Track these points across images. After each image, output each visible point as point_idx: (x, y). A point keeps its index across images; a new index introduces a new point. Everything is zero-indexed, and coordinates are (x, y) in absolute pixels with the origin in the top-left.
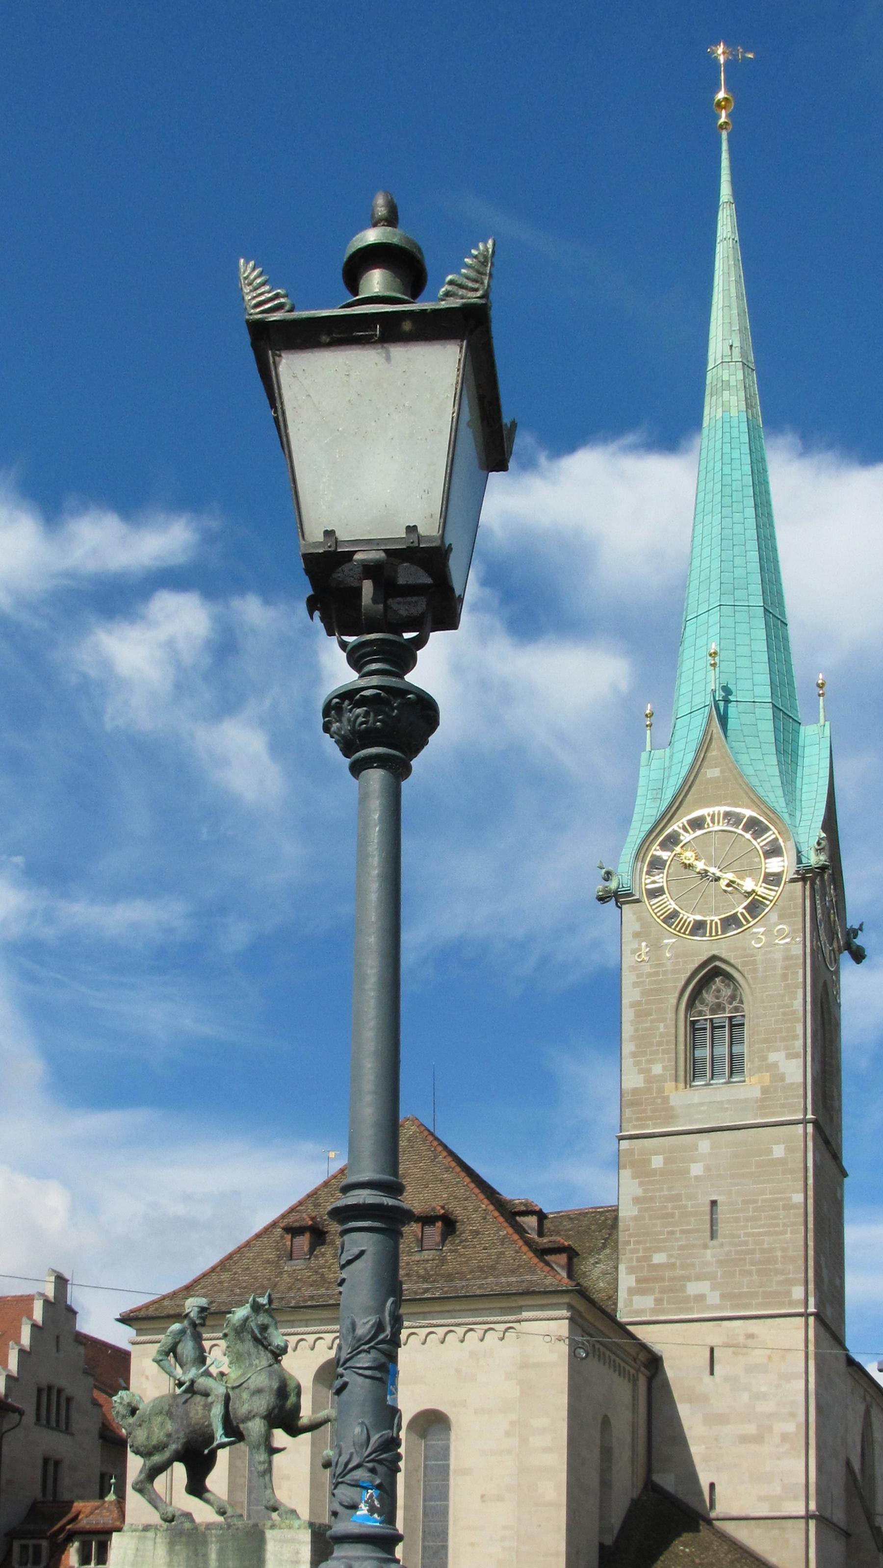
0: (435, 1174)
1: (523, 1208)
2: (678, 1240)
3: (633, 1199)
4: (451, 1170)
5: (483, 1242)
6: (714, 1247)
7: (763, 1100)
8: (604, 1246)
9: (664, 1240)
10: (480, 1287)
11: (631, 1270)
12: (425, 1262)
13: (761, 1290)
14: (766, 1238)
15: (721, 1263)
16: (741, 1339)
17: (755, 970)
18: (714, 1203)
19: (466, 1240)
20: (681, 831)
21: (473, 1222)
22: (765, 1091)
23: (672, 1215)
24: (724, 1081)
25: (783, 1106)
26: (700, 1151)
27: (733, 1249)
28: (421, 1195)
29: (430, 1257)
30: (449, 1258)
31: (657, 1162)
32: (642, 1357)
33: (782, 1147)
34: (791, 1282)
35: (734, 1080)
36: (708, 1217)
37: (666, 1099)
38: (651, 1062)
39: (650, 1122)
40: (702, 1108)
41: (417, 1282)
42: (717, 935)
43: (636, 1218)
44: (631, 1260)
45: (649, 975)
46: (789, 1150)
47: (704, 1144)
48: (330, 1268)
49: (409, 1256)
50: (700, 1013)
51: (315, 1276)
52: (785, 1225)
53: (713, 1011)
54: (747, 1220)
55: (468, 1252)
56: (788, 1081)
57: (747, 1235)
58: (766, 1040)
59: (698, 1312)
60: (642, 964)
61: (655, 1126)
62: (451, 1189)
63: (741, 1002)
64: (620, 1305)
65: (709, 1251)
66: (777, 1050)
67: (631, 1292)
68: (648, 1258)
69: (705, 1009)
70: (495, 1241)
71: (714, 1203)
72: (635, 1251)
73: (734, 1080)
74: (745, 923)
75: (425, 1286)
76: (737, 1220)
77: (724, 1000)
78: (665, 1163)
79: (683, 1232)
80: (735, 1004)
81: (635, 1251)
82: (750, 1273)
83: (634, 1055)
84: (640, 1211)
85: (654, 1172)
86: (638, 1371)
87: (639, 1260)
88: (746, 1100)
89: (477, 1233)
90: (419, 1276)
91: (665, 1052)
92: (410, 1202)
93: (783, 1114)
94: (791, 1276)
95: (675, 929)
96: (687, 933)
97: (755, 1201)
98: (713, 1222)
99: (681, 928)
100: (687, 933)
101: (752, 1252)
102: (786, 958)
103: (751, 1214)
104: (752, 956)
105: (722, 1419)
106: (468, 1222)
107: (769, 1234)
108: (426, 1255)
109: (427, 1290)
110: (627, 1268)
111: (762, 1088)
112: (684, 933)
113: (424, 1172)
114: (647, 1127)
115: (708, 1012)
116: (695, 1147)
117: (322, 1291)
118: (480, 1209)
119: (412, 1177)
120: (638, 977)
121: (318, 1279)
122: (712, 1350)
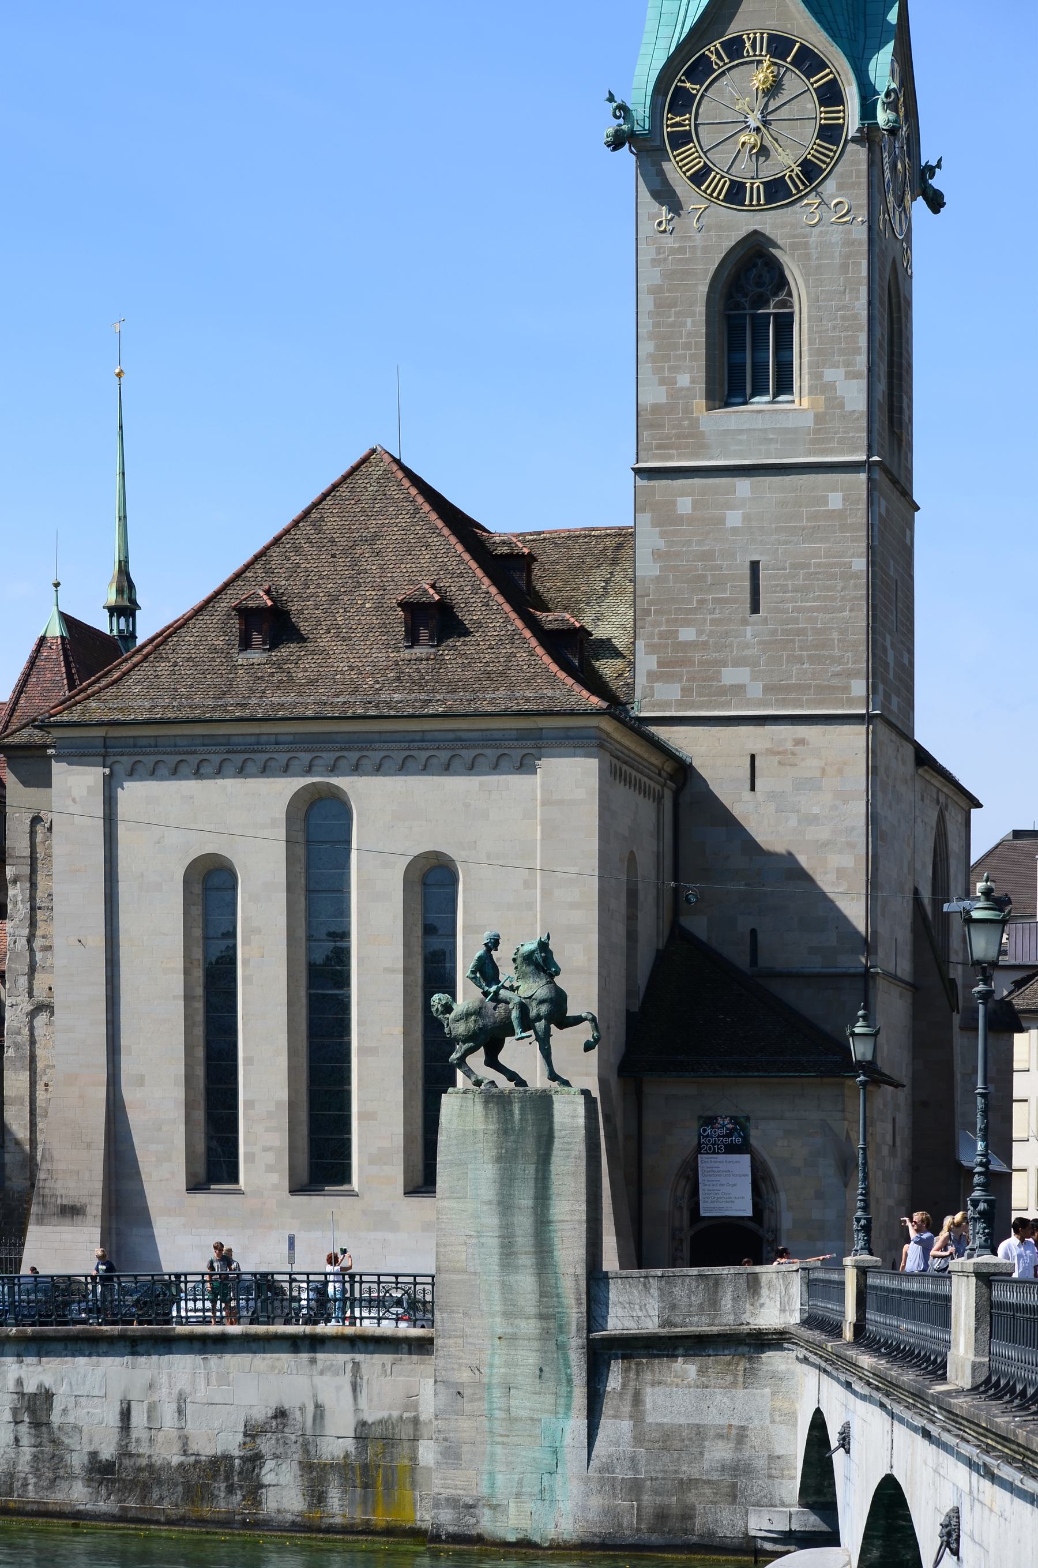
0: (418, 536)
1: (506, 550)
3: (653, 553)
4: (438, 531)
5: (487, 638)
6: (755, 623)
7: (817, 431)
8: (606, 594)
9: (693, 611)
11: (651, 649)
12: (418, 663)
13: (814, 683)
14: (821, 615)
16: (789, 745)
18: (755, 566)
20: (714, 58)
21: (473, 609)
22: (819, 418)
23: (701, 578)
27: (779, 628)
28: (403, 566)
29: (424, 656)
30: (447, 658)
31: (684, 505)
32: (669, 767)
33: (840, 495)
34: (850, 674)
36: (747, 583)
37: (695, 423)
38: (674, 369)
39: (675, 452)
40: (740, 437)
41: (412, 691)
42: (759, 205)
43: (658, 580)
44: (651, 636)
45: (673, 251)
47: (743, 485)
48: (297, 663)
49: (398, 652)
50: (738, 306)
51: (279, 674)
52: (843, 598)
55: (470, 650)
56: (848, 408)
57: (796, 609)
59: (736, 708)
60: (663, 235)
62: (440, 560)
64: (638, 694)
65: (749, 628)
67: (651, 676)
69: (743, 300)
70: (503, 638)
73: (780, 398)
74: (794, 192)
75: (423, 696)
78: (694, 508)
80: (782, 296)
81: (656, 624)
83: (653, 358)
85: (680, 520)
86: (664, 785)
87: (661, 635)
88: (795, 430)
91: (693, 358)
92: (389, 575)
95: (705, 192)
96: (721, 197)
99: (713, 191)
100: (721, 197)
101: (801, 632)
102: (849, 243)
103: (801, 582)
104: (805, 236)
106: (465, 609)
107: (825, 610)
108: (419, 651)
109: (426, 703)
112: (717, 198)
113: (403, 532)
114: (670, 458)
115: (747, 305)
116: (732, 490)
117: (292, 697)
118: (480, 591)
119: (387, 538)
120: (658, 253)
121: (285, 679)
122: (753, 757)
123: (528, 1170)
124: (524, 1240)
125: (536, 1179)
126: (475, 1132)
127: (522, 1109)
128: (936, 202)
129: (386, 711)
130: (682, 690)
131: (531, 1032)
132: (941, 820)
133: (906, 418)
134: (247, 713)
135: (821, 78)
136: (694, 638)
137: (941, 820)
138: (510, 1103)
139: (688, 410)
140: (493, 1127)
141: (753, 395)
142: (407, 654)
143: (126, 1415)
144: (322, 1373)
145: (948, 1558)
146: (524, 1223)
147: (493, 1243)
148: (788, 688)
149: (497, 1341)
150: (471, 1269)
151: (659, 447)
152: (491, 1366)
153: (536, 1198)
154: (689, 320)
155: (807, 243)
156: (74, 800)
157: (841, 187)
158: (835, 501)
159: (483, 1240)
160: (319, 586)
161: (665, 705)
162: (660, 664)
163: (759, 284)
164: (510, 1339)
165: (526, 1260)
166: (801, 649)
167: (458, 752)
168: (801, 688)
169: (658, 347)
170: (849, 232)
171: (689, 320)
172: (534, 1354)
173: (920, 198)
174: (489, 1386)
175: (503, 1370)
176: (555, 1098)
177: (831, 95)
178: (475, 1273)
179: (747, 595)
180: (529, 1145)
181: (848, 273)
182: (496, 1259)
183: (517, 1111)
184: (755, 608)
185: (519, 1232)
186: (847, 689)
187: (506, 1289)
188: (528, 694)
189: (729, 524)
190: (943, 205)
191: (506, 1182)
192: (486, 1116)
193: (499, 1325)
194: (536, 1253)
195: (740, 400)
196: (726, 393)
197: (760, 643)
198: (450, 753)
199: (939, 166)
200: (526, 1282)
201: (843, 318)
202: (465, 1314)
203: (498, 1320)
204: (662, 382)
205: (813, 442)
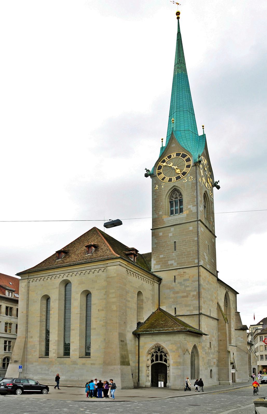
6: (175, 252)
7: (187, 217)
47: (172, 229)
54: (183, 245)
65: (174, 253)
71: (175, 242)
76: (181, 245)
80: (180, 196)
82: (184, 258)
93: (192, 220)
97: (185, 241)
98: (175, 247)
101: (184, 253)
105: (178, 293)
111: (187, 214)
122: (175, 276)
128: (218, 188)
136: (163, 257)
148: (182, 263)
166: (184, 256)
168: (185, 263)
184: (175, 250)
186: (194, 262)
189: (169, 236)
190: (220, 188)
196: (170, 215)
197: (176, 256)
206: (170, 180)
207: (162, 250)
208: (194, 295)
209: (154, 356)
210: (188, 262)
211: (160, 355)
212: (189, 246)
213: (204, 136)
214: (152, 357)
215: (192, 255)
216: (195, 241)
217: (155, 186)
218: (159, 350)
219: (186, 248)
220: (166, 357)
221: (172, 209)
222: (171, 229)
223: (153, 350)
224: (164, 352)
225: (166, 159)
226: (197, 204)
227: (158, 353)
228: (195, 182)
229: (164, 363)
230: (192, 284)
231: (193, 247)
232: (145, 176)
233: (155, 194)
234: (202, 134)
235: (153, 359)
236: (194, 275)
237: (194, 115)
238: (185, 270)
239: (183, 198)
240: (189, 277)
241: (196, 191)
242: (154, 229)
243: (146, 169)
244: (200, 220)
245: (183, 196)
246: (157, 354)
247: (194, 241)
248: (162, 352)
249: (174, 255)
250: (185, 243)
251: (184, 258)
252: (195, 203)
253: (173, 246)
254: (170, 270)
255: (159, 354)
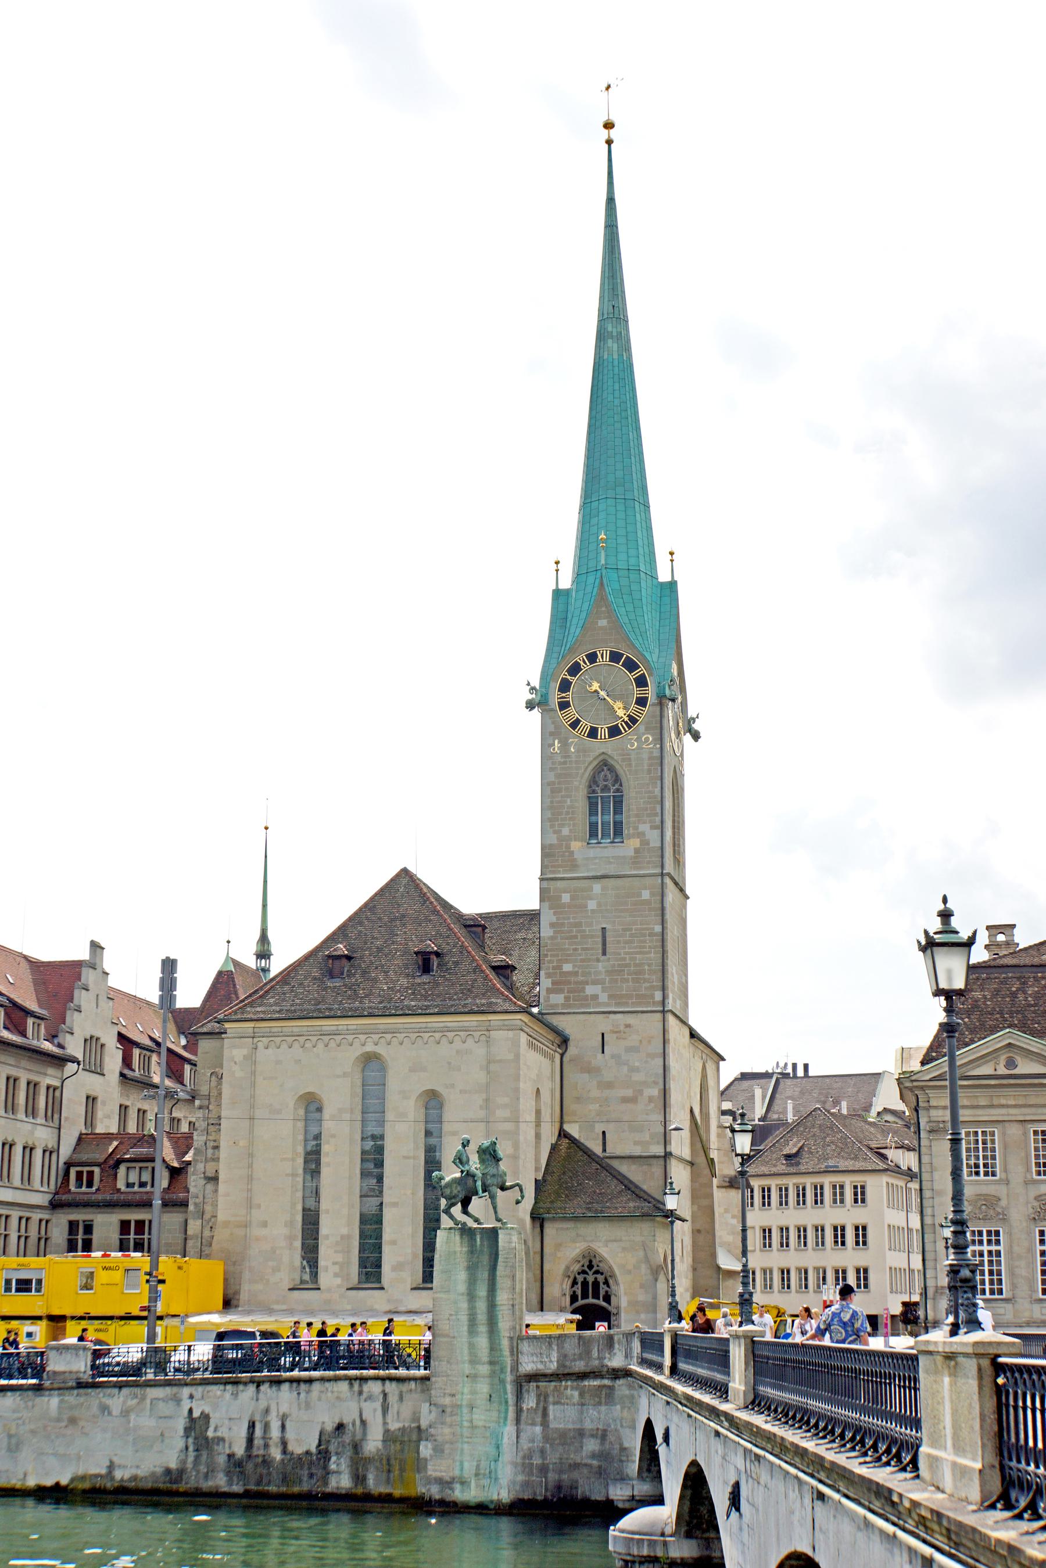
2: (580, 955)
6: (603, 961)
7: (635, 857)
10: (464, 1006)
11: (548, 976)
15: (609, 973)
17: (630, 765)
19: (449, 969)
22: (637, 851)
23: (576, 937)
24: (609, 841)
25: (649, 862)
26: (594, 892)
29: (428, 981)
31: (566, 898)
35: (616, 840)
43: (552, 938)
46: (652, 894)
47: (597, 887)
52: (650, 947)
53: (603, 791)
54: (626, 942)
57: (626, 953)
58: (637, 816)
61: (565, 872)
63: (621, 785)
66: (644, 823)
67: (549, 991)
68: (560, 967)
71: (604, 929)
72: (550, 962)
73: (616, 840)
77: (609, 783)
79: (583, 949)
80: (617, 786)
81: (550, 962)
82: (627, 980)
84: (555, 932)
87: (554, 968)
88: (624, 857)
89: (456, 963)
90: (422, 995)
94: (654, 984)
97: (631, 929)
102: (650, 758)
104: (628, 755)
110: (546, 974)
114: (559, 872)
122: (603, 1034)
123: (484, 1275)
124: (482, 1317)
125: (489, 1280)
126: (455, 1252)
127: (481, 1239)
128: (696, 736)
129: (407, 1012)
130: (565, 997)
131: (487, 1194)
132: (704, 1068)
133: (682, 850)
134: (332, 1013)
135: (637, 673)
137: (704, 1068)
138: (475, 1235)
139: (568, 847)
140: (465, 1249)
141: (602, 839)
142: (418, 980)
143: (252, 1426)
144: (365, 1401)
145: (734, 1514)
146: (482, 1306)
147: (464, 1318)
149: (466, 1379)
150: (452, 1335)
151: (552, 866)
152: (462, 1394)
153: (488, 1291)
154: (569, 800)
155: (630, 759)
156: (235, 1063)
157: (647, 729)
158: (646, 895)
159: (459, 1317)
160: (372, 943)
161: (557, 1005)
162: (553, 983)
163: (605, 780)
164: (473, 1377)
165: (483, 1329)
166: (628, 975)
167: (445, 1034)
169: (553, 814)
170: (652, 753)
171: (569, 800)
172: (486, 1386)
173: (688, 734)
174: (460, 1406)
175: (469, 1397)
176: (499, 1231)
177: (641, 682)
178: (454, 1337)
179: (600, 946)
180: (485, 1260)
181: (650, 774)
182: (466, 1328)
183: (478, 1240)
184: (604, 953)
185: (479, 1311)
187: (471, 1346)
188: (483, 1001)
191: (472, 1282)
192: (461, 1243)
193: (467, 1369)
194: (488, 1324)
195: (595, 841)
198: (441, 1034)
199: (697, 717)
200: (482, 1341)
201: (649, 798)
202: (448, 1362)
203: (466, 1365)
204: (555, 832)
205: (633, 863)
206: (593, 733)
207: (568, 949)
208: (653, 1096)
209: (577, 1284)
210: (638, 996)
211: (593, 1283)
212: (640, 947)
213: (672, 585)
214: (573, 1286)
215: (647, 976)
216: (656, 935)
217: (552, 742)
218: (590, 1267)
219: (632, 953)
220: (608, 1286)
221: (593, 818)
222: (594, 886)
223: (577, 1267)
224: (602, 1274)
225: (582, 663)
226: (662, 822)
227: (587, 1273)
228: (657, 753)
229: (604, 1304)
230: (646, 1062)
231: (650, 952)
232: (527, 707)
233: (551, 768)
234: (670, 579)
235: (574, 1292)
236: (652, 1037)
237: (649, 507)
238: (630, 1019)
239: (625, 793)
240: (641, 1041)
241: (659, 782)
242: (547, 879)
243: (528, 684)
244: (669, 874)
245: (623, 785)
246: (585, 1279)
247: (651, 935)
248: (597, 1272)
249: (600, 968)
250: (631, 935)
251: (627, 980)
252: (658, 819)
253: (600, 940)
254: (590, 1013)
255: (591, 1279)
